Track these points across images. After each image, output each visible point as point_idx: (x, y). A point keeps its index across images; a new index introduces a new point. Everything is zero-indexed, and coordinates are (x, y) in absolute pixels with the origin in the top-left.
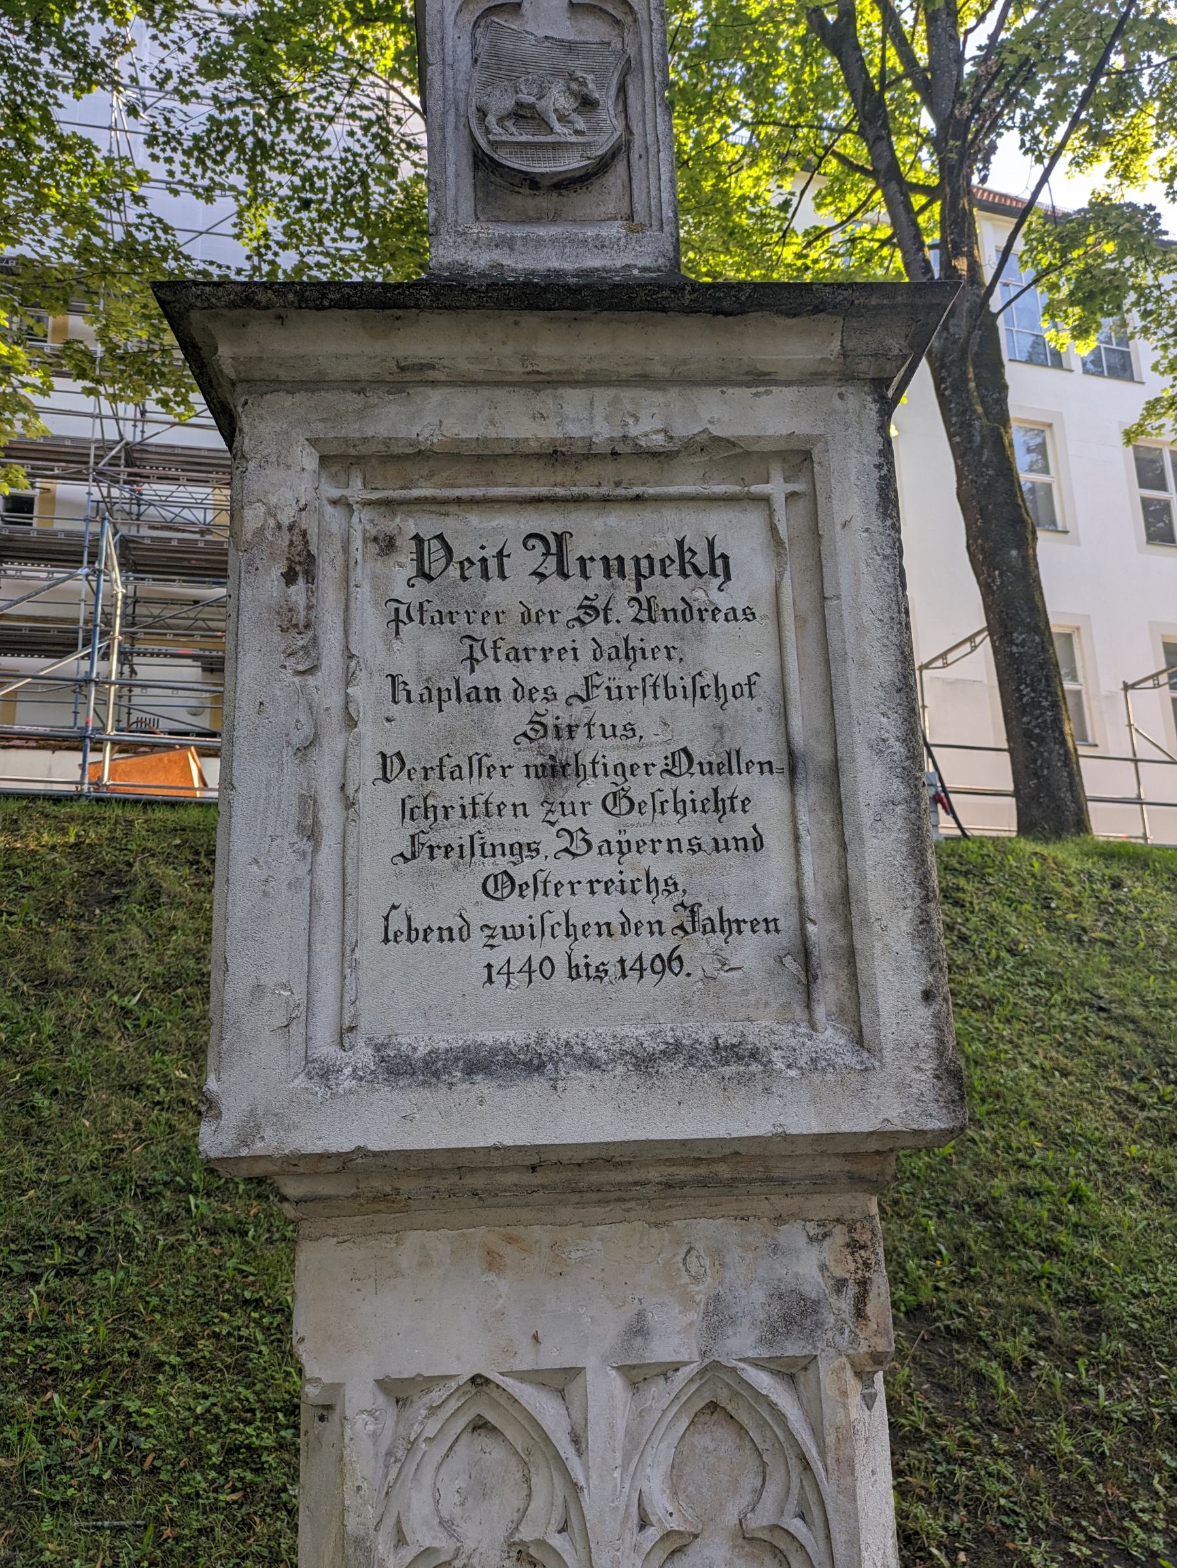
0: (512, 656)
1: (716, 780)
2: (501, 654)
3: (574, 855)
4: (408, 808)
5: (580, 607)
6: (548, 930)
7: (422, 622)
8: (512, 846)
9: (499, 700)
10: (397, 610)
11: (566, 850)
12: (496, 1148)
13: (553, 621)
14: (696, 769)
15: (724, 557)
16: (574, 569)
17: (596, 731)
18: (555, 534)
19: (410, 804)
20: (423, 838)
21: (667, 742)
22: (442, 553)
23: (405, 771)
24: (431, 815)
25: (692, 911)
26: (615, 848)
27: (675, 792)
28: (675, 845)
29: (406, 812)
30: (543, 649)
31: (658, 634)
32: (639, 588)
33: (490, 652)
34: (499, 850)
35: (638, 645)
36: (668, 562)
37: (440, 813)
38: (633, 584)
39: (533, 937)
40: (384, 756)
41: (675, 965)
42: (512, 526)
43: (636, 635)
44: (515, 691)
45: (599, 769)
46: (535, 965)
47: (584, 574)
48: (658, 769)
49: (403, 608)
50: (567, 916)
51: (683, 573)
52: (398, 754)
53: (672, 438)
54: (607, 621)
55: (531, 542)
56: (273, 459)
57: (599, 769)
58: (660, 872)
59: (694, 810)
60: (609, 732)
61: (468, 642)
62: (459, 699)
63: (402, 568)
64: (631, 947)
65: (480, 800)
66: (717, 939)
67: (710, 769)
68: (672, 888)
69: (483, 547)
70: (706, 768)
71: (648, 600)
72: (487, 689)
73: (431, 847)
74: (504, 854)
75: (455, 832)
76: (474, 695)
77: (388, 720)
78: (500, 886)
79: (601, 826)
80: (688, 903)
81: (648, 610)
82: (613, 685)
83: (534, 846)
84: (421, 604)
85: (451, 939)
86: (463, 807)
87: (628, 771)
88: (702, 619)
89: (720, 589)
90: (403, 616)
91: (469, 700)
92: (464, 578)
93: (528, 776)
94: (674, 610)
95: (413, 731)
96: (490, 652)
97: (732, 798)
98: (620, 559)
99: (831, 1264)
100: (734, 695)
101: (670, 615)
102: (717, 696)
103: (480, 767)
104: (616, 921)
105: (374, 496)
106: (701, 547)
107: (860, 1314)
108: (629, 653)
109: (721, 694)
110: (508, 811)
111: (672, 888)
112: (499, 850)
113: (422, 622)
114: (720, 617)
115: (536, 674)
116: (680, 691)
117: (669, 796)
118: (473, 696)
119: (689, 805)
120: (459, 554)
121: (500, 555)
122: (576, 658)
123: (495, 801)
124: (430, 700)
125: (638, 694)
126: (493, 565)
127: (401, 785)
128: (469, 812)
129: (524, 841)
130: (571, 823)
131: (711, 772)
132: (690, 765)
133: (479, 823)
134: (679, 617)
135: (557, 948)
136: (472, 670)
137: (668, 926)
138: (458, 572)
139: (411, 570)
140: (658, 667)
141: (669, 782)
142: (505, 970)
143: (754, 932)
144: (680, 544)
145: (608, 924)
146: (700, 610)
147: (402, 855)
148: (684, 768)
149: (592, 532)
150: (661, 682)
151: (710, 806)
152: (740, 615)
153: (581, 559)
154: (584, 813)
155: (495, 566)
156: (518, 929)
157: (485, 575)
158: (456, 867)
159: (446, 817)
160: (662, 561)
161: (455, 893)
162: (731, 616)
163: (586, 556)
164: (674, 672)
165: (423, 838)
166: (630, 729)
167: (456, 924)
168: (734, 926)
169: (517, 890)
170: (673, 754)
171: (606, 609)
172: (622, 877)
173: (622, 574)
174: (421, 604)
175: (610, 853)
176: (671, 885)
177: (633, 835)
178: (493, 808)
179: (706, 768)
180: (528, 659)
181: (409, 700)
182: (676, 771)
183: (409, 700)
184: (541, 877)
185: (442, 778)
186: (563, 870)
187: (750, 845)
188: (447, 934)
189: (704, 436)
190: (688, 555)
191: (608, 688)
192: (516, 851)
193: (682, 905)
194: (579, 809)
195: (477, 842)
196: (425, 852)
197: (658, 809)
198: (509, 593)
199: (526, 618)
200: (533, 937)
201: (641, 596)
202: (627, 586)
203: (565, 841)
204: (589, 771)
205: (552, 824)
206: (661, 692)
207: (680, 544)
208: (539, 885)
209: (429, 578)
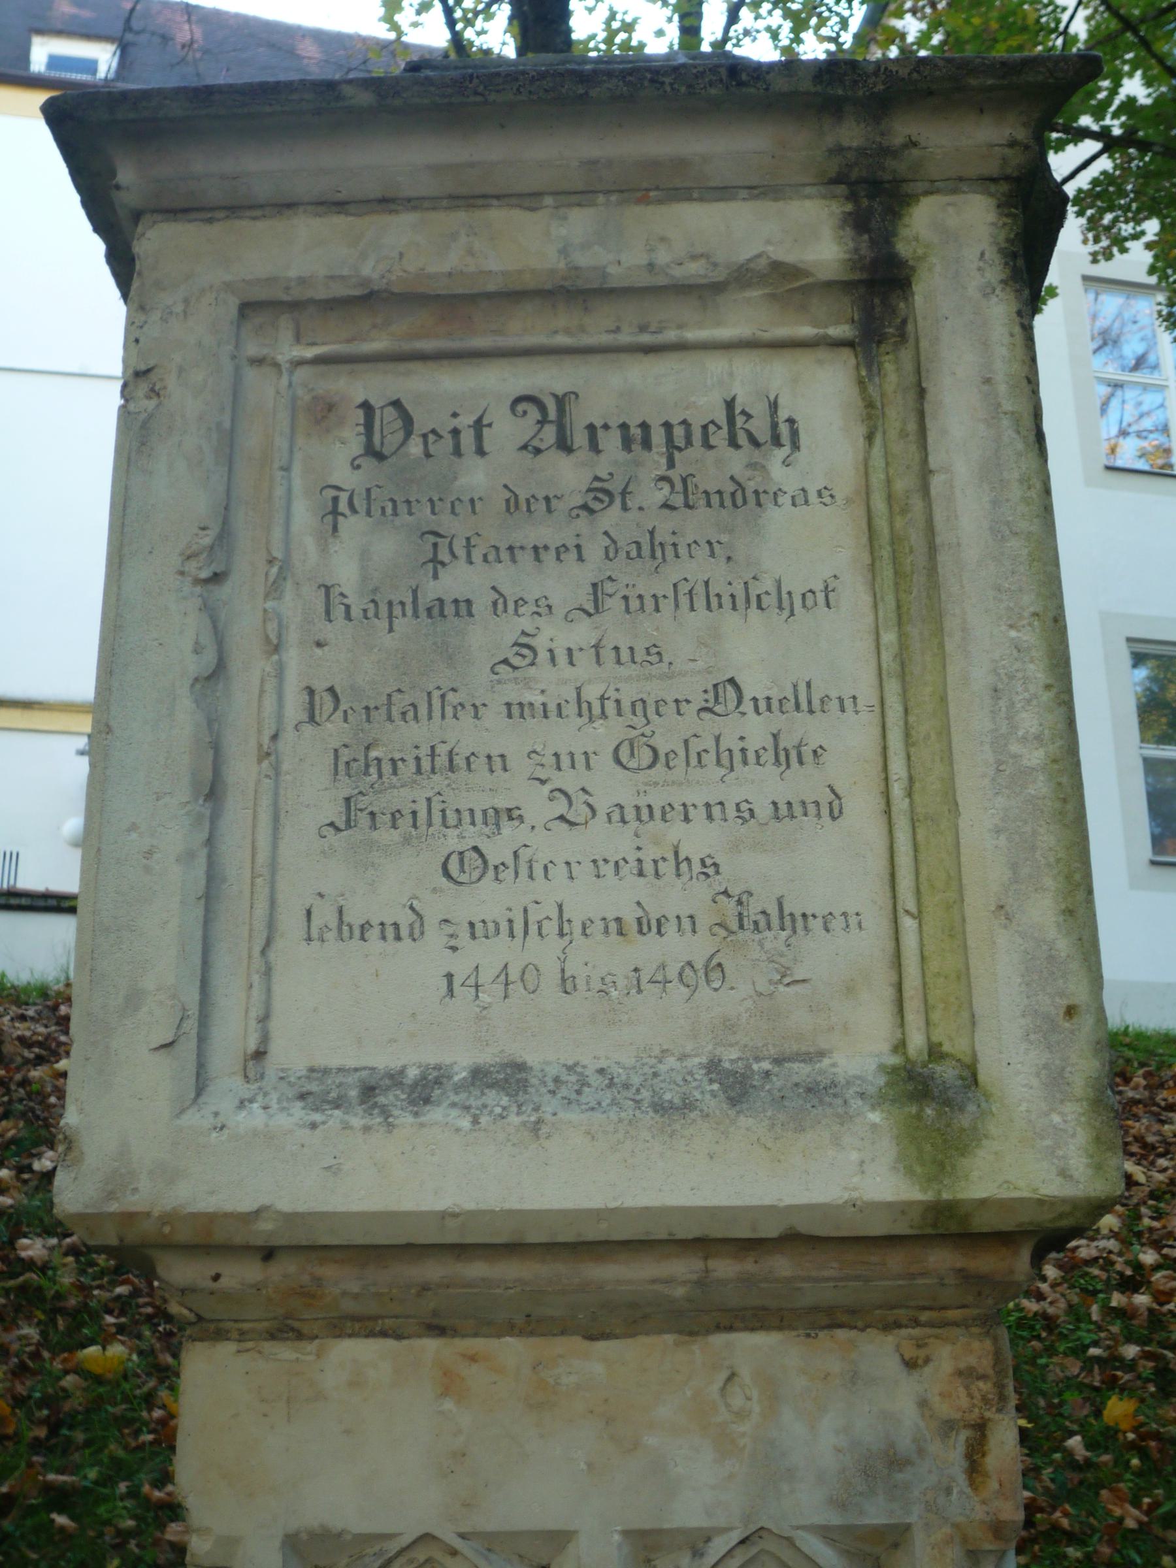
0: (491, 558)
1: (777, 721)
2: (477, 555)
3: (572, 824)
4: (343, 759)
5: (589, 490)
6: (533, 928)
7: (369, 513)
8: (485, 812)
9: (470, 614)
10: (335, 500)
11: (562, 818)
12: (455, 1215)
13: (549, 510)
14: (748, 706)
15: (791, 421)
16: (580, 439)
17: (608, 655)
18: (555, 396)
19: (345, 755)
20: (363, 802)
21: (708, 671)
22: (399, 424)
23: (339, 714)
24: (373, 770)
25: (740, 902)
26: (630, 814)
27: (717, 739)
28: (716, 811)
29: (340, 766)
30: (536, 548)
31: (697, 524)
32: (671, 464)
33: (460, 552)
34: (466, 817)
35: (669, 539)
36: (712, 428)
37: (387, 768)
38: (664, 461)
39: (512, 935)
40: (311, 692)
41: (715, 975)
42: (497, 382)
43: (665, 525)
44: (495, 604)
45: (610, 706)
46: (514, 975)
47: (594, 447)
48: (694, 707)
49: (344, 497)
50: (560, 906)
51: (733, 443)
52: (331, 690)
53: (715, 265)
54: (625, 508)
55: (520, 408)
56: (179, 308)
57: (610, 706)
58: (693, 849)
59: (745, 762)
60: (625, 655)
61: (432, 539)
62: (416, 615)
64: (647, 951)
65: (442, 750)
66: (775, 939)
68: (711, 871)
69: (455, 415)
70: (762, 705)
71: (684, 480)
72: (456, 601)
73: (372, 814)
74: (473, 823)
76: (437, 609)
77: (319, 645)
79: (612, 787)
80: (735, 891)
81: (685, 495)
82: (632, 594)
83: (516, 813)
84: (368, 490)
85: (398, 938)
86: (418, 759)
87: (651, 710)
88: (759, 504)
89: (786, 463)
90: (343, 506)
91: (430, 616)
92: (428, 455)
93: (510, 716)
94: (719, 492)
96: (460, 552)
97: (798, 747)
98: (644, 426)
99: (935, 1400)
100: (804, 606)
101: (715, 499)
102: (781, 608)
104: (630, 916)
105: (310, 353)
106: (760, 410)
108: (654, 550)
109: (786, 604)
110: (480, 763)
111: (711, 871)
112: (466, 817)
113: (369, 513)
114: (785, 500)
116: (727, 600)
117: (710, 744)
118: (436, 611)
119: (738, 757)
120: (422, 423)
121: (479, 425)
122: (580, 558)
123: (463, 751)
124: (376, 616)
125: (667, 606)
126: (468, 439)
127: (335, 730)
128: (426, 764)
129: (502, 803)
130: (568, 780)
131: (769, 709)
132: (740, 702)
134: (728, 502)
135: (544, 953)
136: (436, 576)
137: (703, 922)
138: (421, 447)
139: (356, 446)
140: (696, 569)
142: (472, 981)
143: (827, 930)
144: (730, 405)
145: (618, 920)
146: (756, 492)
147: (332, 824)
148: (732, 705)
149: (608, 391)
150: (700, 589)
151: (768, 757)
152: (813, 497)
153: (591, 428)
154: (588, 767)
156: (491, 926)
157: (457, 452)
158: (407, 840)
159: (395, 773)
160: (705, 428)
162: (800, 500)
163: (598, 423)
164: (718, 574)
165: (363, 802)
166: (655, 651)
167: (405, 918)
168: (800, 923)
169: (491, 873)
170: (715, 686)
171: (624, 493)
172: (640, 855)
173: (647, 444)
174: (368, 490)
175: (623, 821)
176: (710, 867)
177: (657, 799)
178: (459, 761)
179: (762, 705)
180: (514, 560)
181: (348, 617)
182: (717, 709)
183: (348, 617)
184: (525, 854)
185: (390, 718)
187: (825, 811)
189: (763, 262)
190: (740, 421)
191: (625, 598)
192: (491, 820)
193: (725, 893)
194: (580, 760)
195: (436, 807)
196: (364, 820)
197: (694, 761)
199: (512, 504)
200: (512, 935)
201: (674, 475)
202: (656, 461)
203: (561, 807)
204: (597, 710)
205: (543, 782)
206: (700, 602)
207: (730, 405)
209: (380, 457)
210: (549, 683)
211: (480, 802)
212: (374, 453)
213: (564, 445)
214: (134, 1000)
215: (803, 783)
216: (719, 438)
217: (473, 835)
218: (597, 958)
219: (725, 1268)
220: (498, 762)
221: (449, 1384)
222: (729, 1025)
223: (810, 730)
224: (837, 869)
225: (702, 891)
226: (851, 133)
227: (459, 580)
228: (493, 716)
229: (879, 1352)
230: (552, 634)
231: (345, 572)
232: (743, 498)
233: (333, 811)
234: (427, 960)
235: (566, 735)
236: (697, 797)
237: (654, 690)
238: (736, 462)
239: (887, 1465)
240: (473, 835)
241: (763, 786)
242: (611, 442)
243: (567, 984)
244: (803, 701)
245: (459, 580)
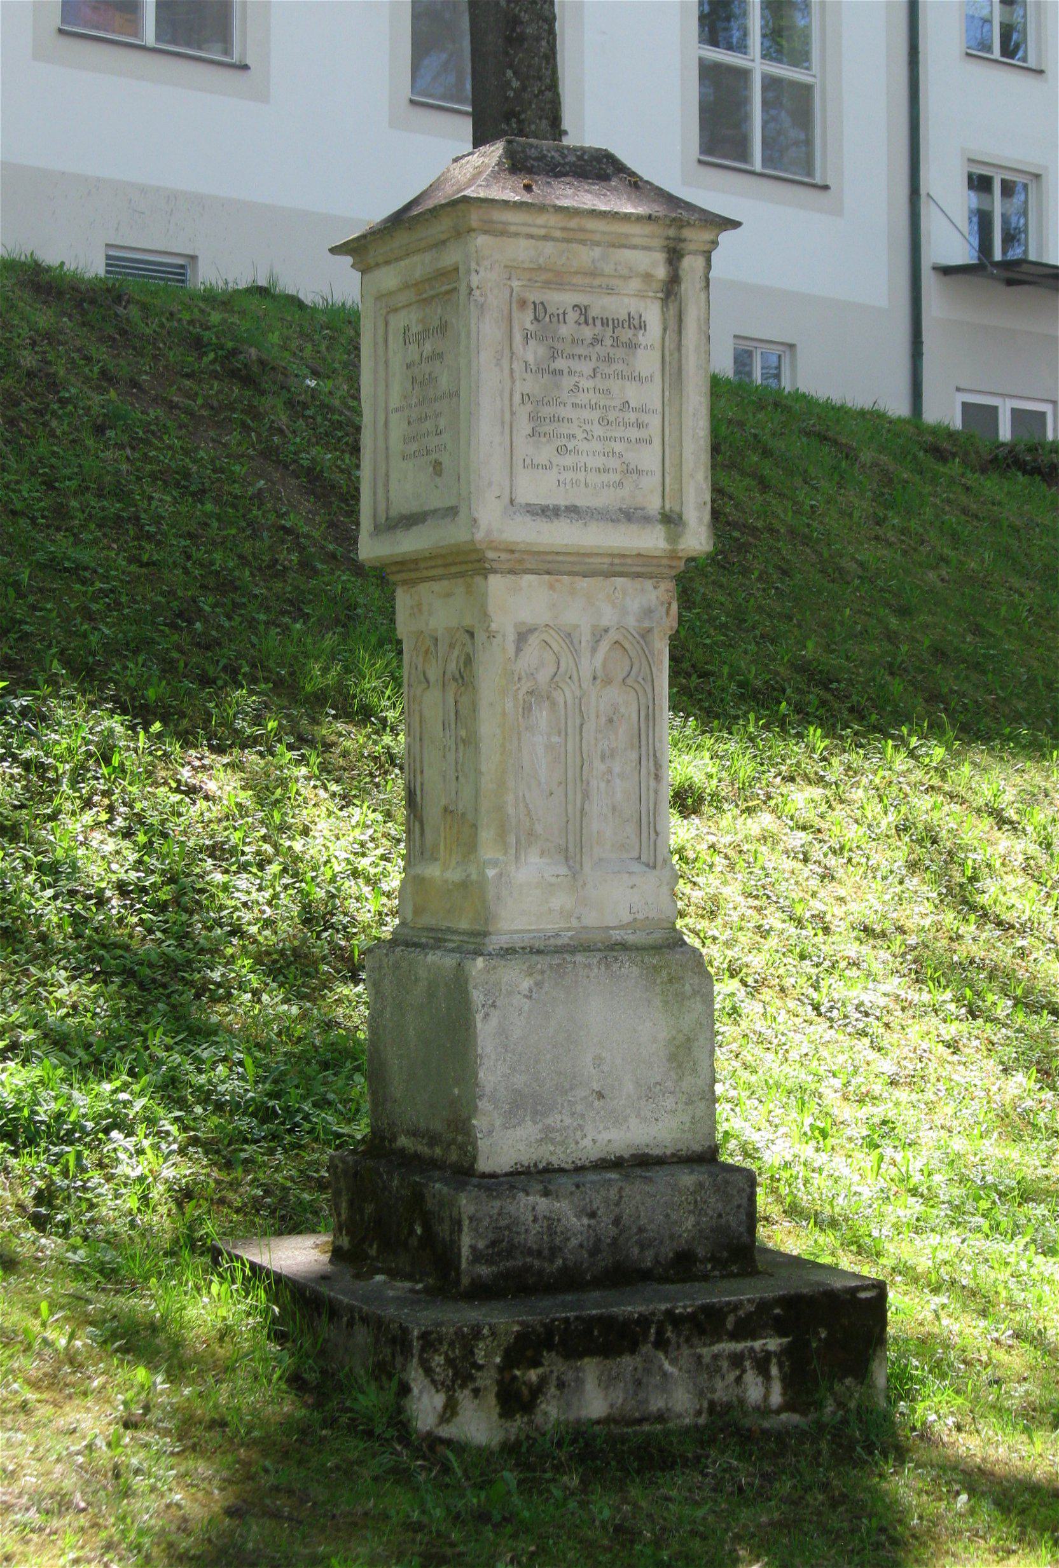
31: (619, 353)
43: (612, 351)
58: (617, 450)
63: (529, 315)
64: (605, 477)
66: (635, 476)
67: (635, 410)
78: (561, 450)
79: (598, 431)
95: (530, 385)
103: (557, 402)
107: (668, 613)
108: (609, 359)
115: (575, 365)
120: (549, 311)
127: (529, 407)
133: (556, 424)
135: (581, 476)
140: (619, 367)
141: (621, 414)
176: (621, 456)
177: (609, 435)
188: (545, 467)
199: (573, 341)
208: (576, 451)
210: (582, 398)
211: (566, 432)
212: (536, 319)
213: (586, 323)
214: (490, 484)
215: (642, 434)
216: (626, 325)
217: (564, 441)
218: (595, 479)
219: (617, 561)
220: (570, 420)
221: (551, 587)
222: (623, 499)
223: (645, 418)
224: (649, 458)
225: (619, 462)
226: (672, 232)
227: (560, 364)
228: (569, 406)
229: (649, 584)
230: (585, 383)
231: (531, 359)
232: (632, 346)
233: (529, 431)
234: (553, 475)
235: (586, 414)
236: (618, 435)
237: (608, 403)
238: (630, 333)
239: (648, 612)
240: (564, 441)
241: (633, 434)
242: (598, 323)
243: (586, 485)
244: (643, 410)
245: (560, 364)
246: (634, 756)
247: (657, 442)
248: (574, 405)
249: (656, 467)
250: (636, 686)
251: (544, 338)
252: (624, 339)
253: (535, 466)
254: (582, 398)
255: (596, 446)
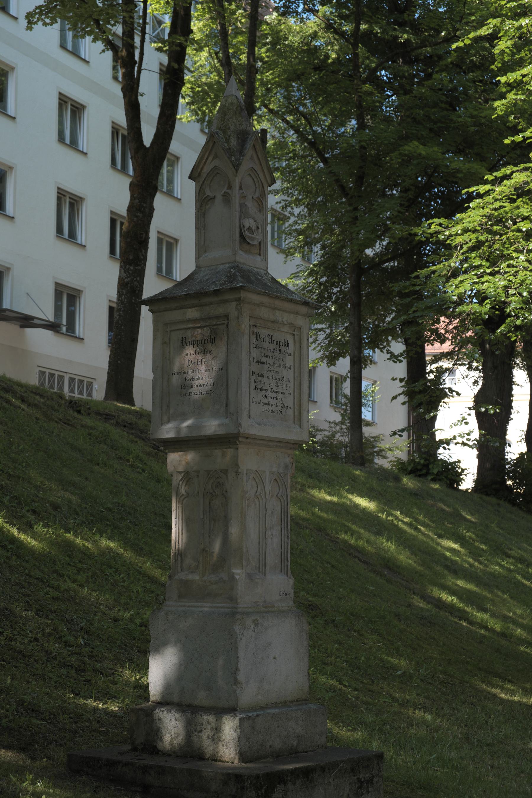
31: (281, 356)
75: (260, 387)
78: (264, 396)
79: (275, 389)
108: (278, 359)
135: (270, 407)
155: (264, 340)
161: (259, 397)
186: (271, 395)
198: (266, 345)
208: (268, 397)
210: (270, 374)
227: (264, 359)
230: (271, 368)
241: (285, 390)
244: (287, 381)
245: (264, 359)
246: (279, 528)
247: (292, 394)
248: (268, 378)
249: (290, 404)
250: (281, 498)
251: (259, 348)
252: (282, 351)
253: (256, 402)
254: (270, 374)
255: (273, 395)
